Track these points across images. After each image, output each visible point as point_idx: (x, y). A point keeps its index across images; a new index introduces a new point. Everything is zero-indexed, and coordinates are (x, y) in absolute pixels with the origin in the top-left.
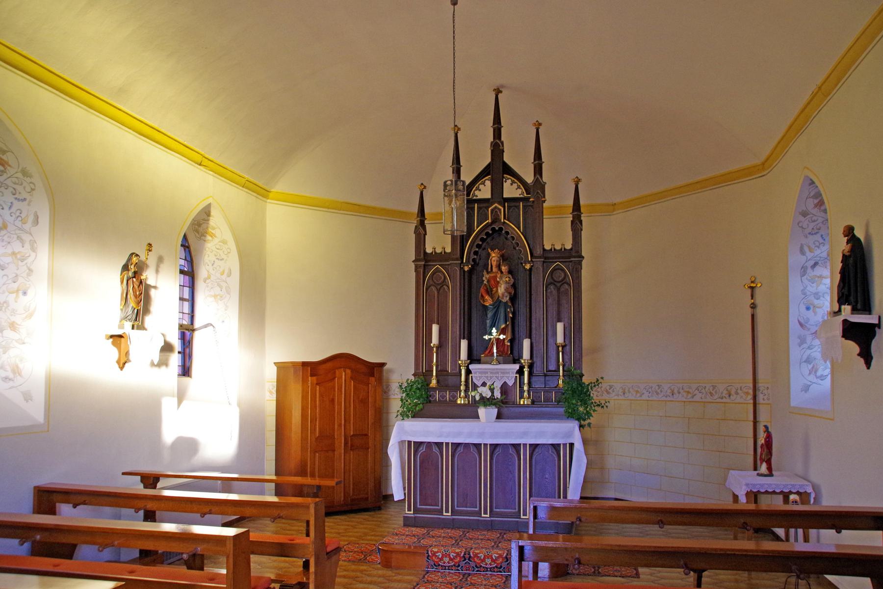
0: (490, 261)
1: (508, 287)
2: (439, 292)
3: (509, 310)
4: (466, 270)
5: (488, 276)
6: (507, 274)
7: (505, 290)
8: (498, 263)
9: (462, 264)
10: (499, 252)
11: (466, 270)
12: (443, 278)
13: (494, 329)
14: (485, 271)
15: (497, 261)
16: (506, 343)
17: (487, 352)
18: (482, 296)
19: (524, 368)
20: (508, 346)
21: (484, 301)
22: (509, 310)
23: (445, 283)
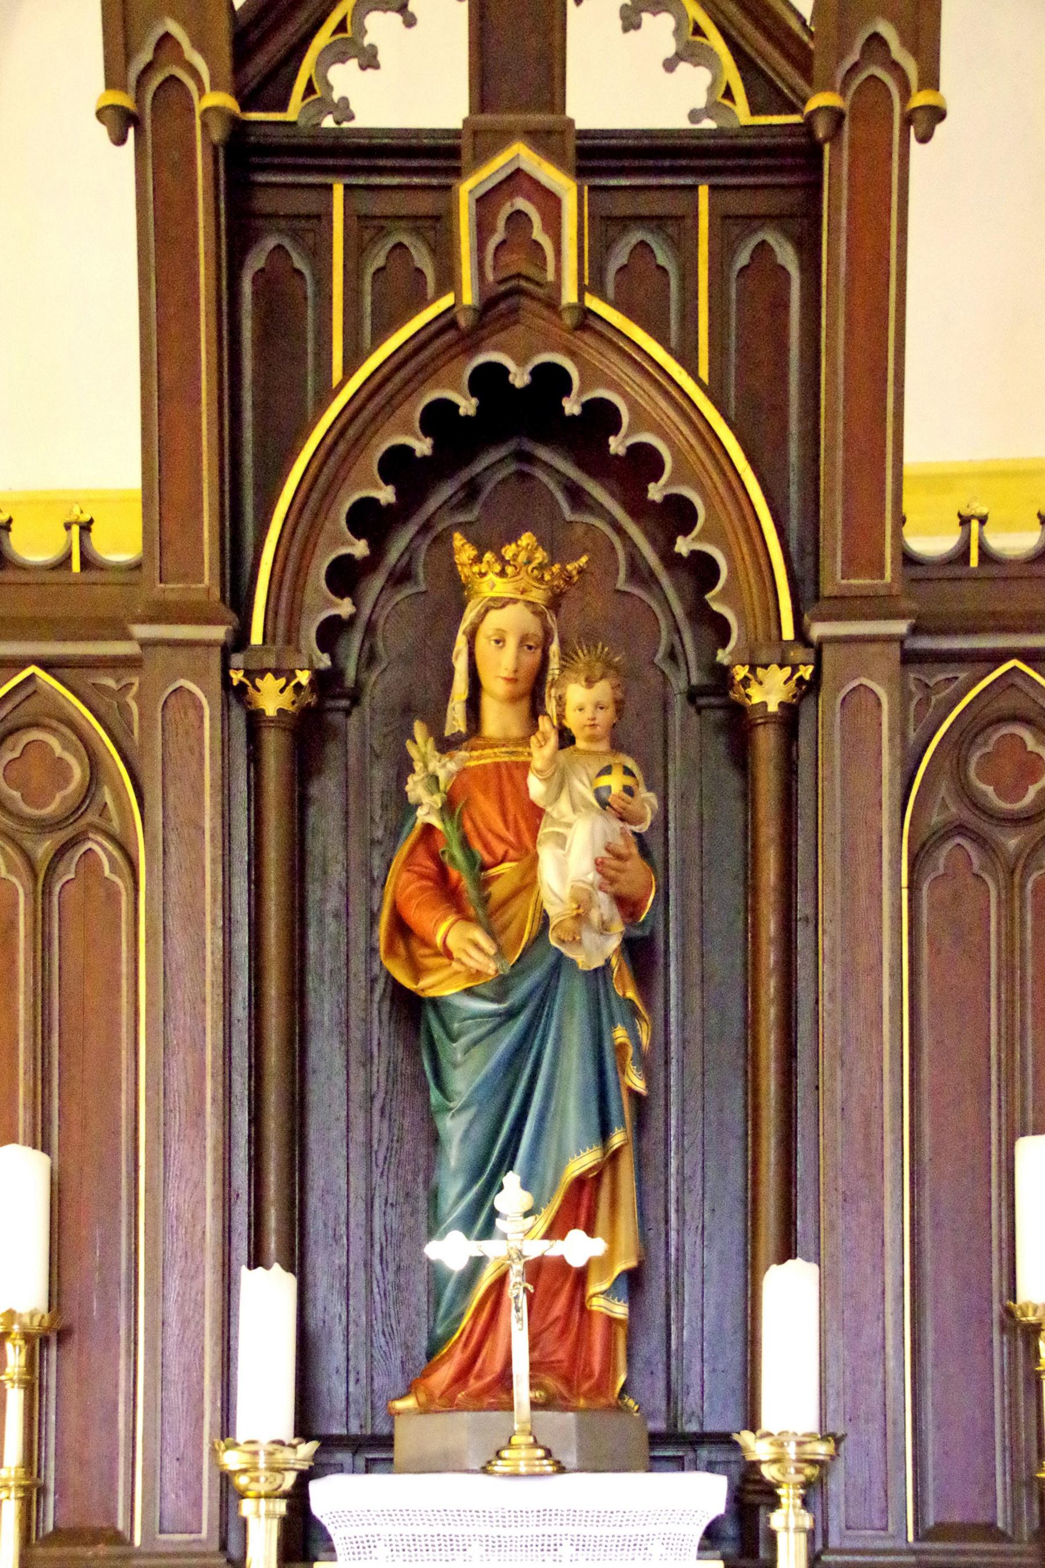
0: (461, 643)
1: (619, 843)
2: (47, 892)
3: (620, 1034)
4: (271, 711)
5: (445, 768)
6: (603, 746)
7: (599, 865)
8: (532, 659)
9: (237, 659)
10: (540, 556)
11: (271, 711)
12: (78, 773)
13: (511, 1180)
14: (419, 729)
15: (523, 641)
16: (597, 1304)
17: (445, 1373)
18: (401, 928)
19: (775, 1503)
20: (611, 1322)
21: (417, 971)
22: (620, 1034)
23: (91, 817)
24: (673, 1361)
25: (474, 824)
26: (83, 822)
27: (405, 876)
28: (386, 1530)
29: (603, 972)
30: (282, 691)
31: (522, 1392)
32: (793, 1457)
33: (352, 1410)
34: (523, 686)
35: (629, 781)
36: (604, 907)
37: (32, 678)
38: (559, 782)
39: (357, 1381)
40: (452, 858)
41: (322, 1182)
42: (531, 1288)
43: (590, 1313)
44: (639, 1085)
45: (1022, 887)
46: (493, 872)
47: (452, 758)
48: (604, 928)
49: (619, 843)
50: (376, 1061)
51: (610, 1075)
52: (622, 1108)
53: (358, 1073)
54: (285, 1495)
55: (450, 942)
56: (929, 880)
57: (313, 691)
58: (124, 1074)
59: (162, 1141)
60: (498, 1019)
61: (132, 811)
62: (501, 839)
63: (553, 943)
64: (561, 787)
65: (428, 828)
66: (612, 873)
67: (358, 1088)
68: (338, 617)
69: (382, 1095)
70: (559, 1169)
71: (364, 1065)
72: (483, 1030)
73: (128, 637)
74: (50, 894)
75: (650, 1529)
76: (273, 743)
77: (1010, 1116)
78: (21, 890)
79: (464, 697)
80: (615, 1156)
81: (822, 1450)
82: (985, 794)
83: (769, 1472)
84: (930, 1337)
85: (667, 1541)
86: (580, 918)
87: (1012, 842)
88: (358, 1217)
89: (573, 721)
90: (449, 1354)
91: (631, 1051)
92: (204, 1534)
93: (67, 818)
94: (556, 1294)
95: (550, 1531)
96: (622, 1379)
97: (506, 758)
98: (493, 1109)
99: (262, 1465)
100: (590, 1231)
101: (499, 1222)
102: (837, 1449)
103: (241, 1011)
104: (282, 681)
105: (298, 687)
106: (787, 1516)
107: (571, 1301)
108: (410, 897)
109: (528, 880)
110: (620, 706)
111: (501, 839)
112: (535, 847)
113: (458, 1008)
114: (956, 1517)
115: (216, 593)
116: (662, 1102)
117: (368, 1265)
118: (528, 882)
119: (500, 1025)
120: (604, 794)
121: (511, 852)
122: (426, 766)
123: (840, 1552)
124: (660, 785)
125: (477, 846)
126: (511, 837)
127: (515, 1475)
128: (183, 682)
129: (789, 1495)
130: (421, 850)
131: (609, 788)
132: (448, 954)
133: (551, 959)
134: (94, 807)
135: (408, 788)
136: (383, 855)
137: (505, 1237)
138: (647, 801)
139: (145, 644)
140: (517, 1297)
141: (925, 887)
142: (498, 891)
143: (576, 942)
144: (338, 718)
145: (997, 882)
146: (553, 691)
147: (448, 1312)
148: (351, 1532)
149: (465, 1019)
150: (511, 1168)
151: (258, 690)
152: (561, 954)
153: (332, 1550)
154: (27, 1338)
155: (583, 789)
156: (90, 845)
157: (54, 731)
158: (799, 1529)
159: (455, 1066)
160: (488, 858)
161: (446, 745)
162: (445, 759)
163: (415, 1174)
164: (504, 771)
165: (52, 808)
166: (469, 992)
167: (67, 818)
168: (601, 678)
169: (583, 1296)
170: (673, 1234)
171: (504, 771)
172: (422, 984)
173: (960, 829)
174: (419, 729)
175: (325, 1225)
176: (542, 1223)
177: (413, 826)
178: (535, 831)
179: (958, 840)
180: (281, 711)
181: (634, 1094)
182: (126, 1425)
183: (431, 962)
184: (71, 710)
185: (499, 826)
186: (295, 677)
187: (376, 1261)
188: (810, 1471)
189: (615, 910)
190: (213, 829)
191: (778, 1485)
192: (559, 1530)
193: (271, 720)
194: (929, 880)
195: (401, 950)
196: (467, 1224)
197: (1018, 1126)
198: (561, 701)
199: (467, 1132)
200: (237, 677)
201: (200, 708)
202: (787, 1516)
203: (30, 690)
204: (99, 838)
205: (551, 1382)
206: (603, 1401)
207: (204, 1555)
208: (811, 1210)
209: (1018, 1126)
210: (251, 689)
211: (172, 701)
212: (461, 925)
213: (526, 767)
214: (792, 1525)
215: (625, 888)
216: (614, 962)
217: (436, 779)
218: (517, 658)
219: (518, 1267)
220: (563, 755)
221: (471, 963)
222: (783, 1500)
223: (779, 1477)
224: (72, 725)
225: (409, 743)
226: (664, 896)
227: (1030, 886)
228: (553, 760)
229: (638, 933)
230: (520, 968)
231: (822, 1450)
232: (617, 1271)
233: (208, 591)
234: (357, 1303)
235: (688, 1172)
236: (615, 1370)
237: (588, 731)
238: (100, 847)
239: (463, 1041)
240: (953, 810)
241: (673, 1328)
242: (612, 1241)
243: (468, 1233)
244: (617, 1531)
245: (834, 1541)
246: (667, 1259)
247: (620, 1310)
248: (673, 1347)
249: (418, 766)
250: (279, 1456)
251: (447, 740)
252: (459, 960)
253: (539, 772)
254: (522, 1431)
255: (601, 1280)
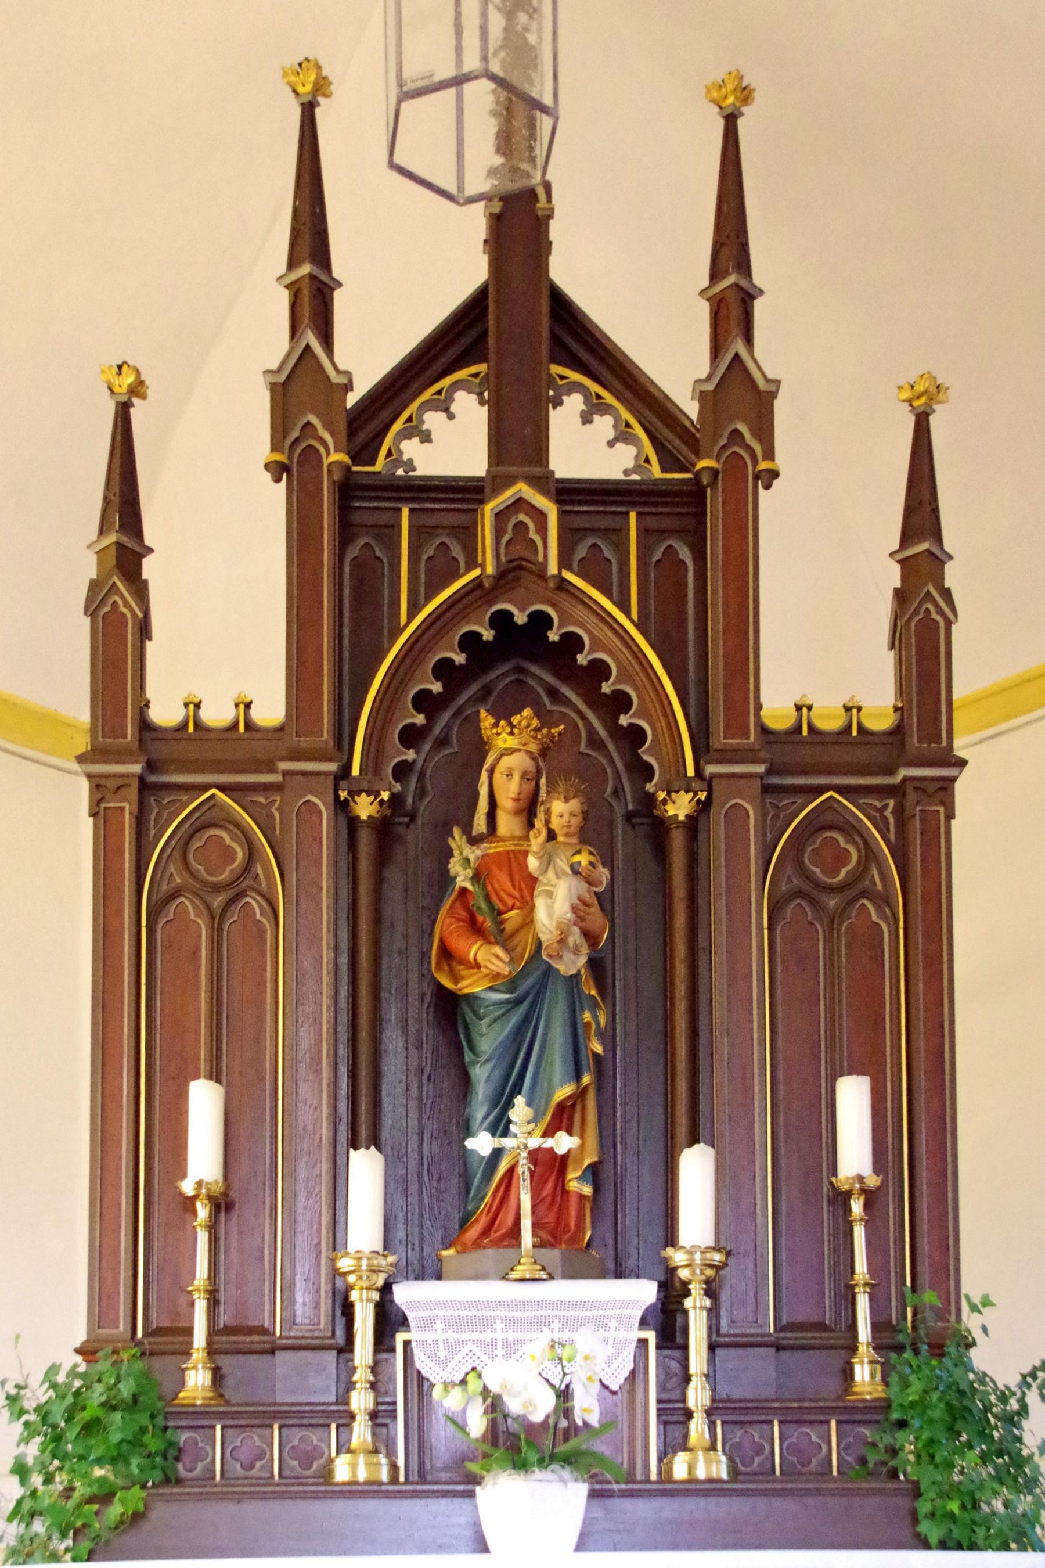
0: (484, 776)
1: (587, 897)
2: (220, 930)
3: (587, 1016)
4: (364, 817)
5: (473, 854)
6: (574, 840)
7: (574, 909)
8: (530, 786)
9: (343, 784)
10: (535, 723)
11: (364, 817)
12: (240, 855)
13: (520, 1101)
14: (457, 832)
15: (524, 775)
16: (573, 1186)
17: (473, 1232)
18: (446, 954)
19: (687, 1293)
20: (582, 1197)
21: (456, 979)
22: (587, 1016)
23: (248, 882)
24: (619, 1238)
25: (493, 887)
26: (244, 885)
27: (448, 921)
28: (441, 1313)
29: (575, 978)
30: (371, 804)
31: (527, 1238)
32: (698, 1262)
33: (410, 1269)
34: (523, 804)
35: (592, 858)
36: (575, 937)
37: (213, 796)
38: (548, 860)
39: (413, 1249)
40: (479, 908)
41: (390, 1122)
42: (532, 1167)
43: (568, 1192)
44: (598, 1048)
45: (839, 930)
46: (505, 916)
47: (478, 848)
48: (576, 951)
49: (587, 897)
50: (425, 1046)
51: (581, 1039)
52: (586, 1061)
53: (413, 1052)
54: (377, 1289)
55: (479, 958)
56: (782, 924)
57: (389, 807)
58: (268, 1043)
59: (293, 1081)
60: (509, 1006)
61: (274, 877)
62: (510, 895)
63: (545, 958)
64: (549, 863)
65: (464, 891)
66: (582, 914)
67: (414, 1063)
68: (405, 761)
69: (428, 1068)
70: (549, 1096)
71: (417, 1048)
72: (499, 1012)
73: (272, 770)
74: (222, 930)
75: (609, 1312)
76: (365, 840)
77: (833, 1062)
78: (203, 927)
79: (486, 810)
80: (585, 1089)
81: (718, 1257)
82: (814, 873)
83: (684, 1274)
84: (783, 1206)
85: (620, 1319)
86: (562, 941)
87: (832, 902)
88: (413, 1144)
89: (555, 823)
90: (477, 1220)
91: (594, 1026)
92: (322, 1326)
93: (233, 883)
94: (546, 1182)
95: (547, 1313)
96: (588, 1234)
97: (513, 848)
98: (504, 1064)
99: (364, 1268)
100: (570, 1133)
101: (512, 1127)
102: (727, 1259)
103: (343, 1004)
104: (372, 798)
105: (382, 801)
106: (695, 1300)
107: (555, 1189)
108: (451, 933)
109: (528, 920)
110: (585, 815)
111: (510, 895)
112: (532, 898)
113: (484, 999)
114: (800, 1318)
115: (331, 742)
116: (611, 1073)
117: (420, 1176)
118: (529, 920)
119: (508, 1011)
120: (576, 867)
121: (517, 904)
122: (461, 853)
123: (728, 1335)
124: (609, 862)
125: (495, 899)
126: (516, 894)
127: (523, 1280)
128: (310, 797)
129: (696, 1289)
130: (458, 905)
131: (579, 863)
132: (478, 966)
133: (543, 967)
134: (250, 876)
135: (450, 866)
136: (429, 916)
137: (515, 1136)
138: (603, 874)
139: (286, 774)
140: (523, 1173)
141: (779, 928)
142: (509, 927)
143: (560, 957)
144: (401, 830)
145: (822, 924)
146: (542, 808)
147: (476, 1195)
148: (420, 1314)
149: (488, 1006)
150: (519, 1093)
151: (356, 803)
152: (550, 965)
153: (408, 1326)
154: (210, 1198)
155: (563, 864)
156: (248, 899)
157: (226, 829)
158: (702, 1308)
159: (482, 1035)
160: (502, 907)
161: (474, 841)
162: (474, 848)
163: (450, 1118)
164: (512, 856)
165: (224, 876)
166: (491, 989)
167: (233, 883)
168: (574, 797)
169: (563, 1182)
170: (619, 1157)
171: (512, 856)
172: (460, 985)
173: (800, 894)
174: (457, 832)
175: (392, 1149)
176: (539, 1131)
177: (453, 890)
178: (532, 891)
179: (798, 901)
180: (370, 817)
181: (596, 1055)
182: (270, 1262)
183: (464, 973)
184: (239, 817)
185: (508, 885)
186: (380, 795)
187: (425, 1173)
188: (710, 1272)
189: (583, 938)
190: (328, 887)
191: (689, 1282)
192: (551, 1313)
193: (364, 822)
194: (782, 924)
195: (446, 968)
196: (493, 1131)
197: (838, 1068)
198: (548, 812)
199: (489, 1077)
200: (343, 795)
201: (320, 812)
202: (695, 1300)
203: (212, 803)
204: (254, 895)
205: (544, 1235)
206: (576, 1246)
207: (323, 1338)
208: (708, 1125)
209: (838, 1068)
210: (352, 804)
211: (303, 808)
212: (485, 947)
213: (526, 853)
214: (698, 1305)
215: (588, 925)
216: (583, 972)
217: (467, 860)
218: (521, 785)
219: (524, 1154)
220: (549, 845)
221: (493, 968)
222: (693, 1291)
223: (690, 1277)
224: (238, 825)
225: (450, 840)
226: (612, 937)
227: (843, 928)
228: (543, 847)
229: (596, 955)
230: (524, 973)
231: (718, 1257)
232: (586, 1163)
233: (326, 741)
234: (413, 1199)
235: (628, 1117)
236: (584, 1228)
237: (565, 830)
238: (254, 902)
239: (487, 1020)
240: (795, 882)
241: (619, 1216)
242: (582, 1137)
243: (494, 1135)
244: (588, 1313)
245: (724, 1329)
246: (616, 1174)
247: (587, 1190)
248: (619, 1229)
249: (456, 853)
250: (375, 1262)
251: (475, 837)
252: (486, 967)
253: (536, 853)
254: (527, 1256)
255: (575, 1170)
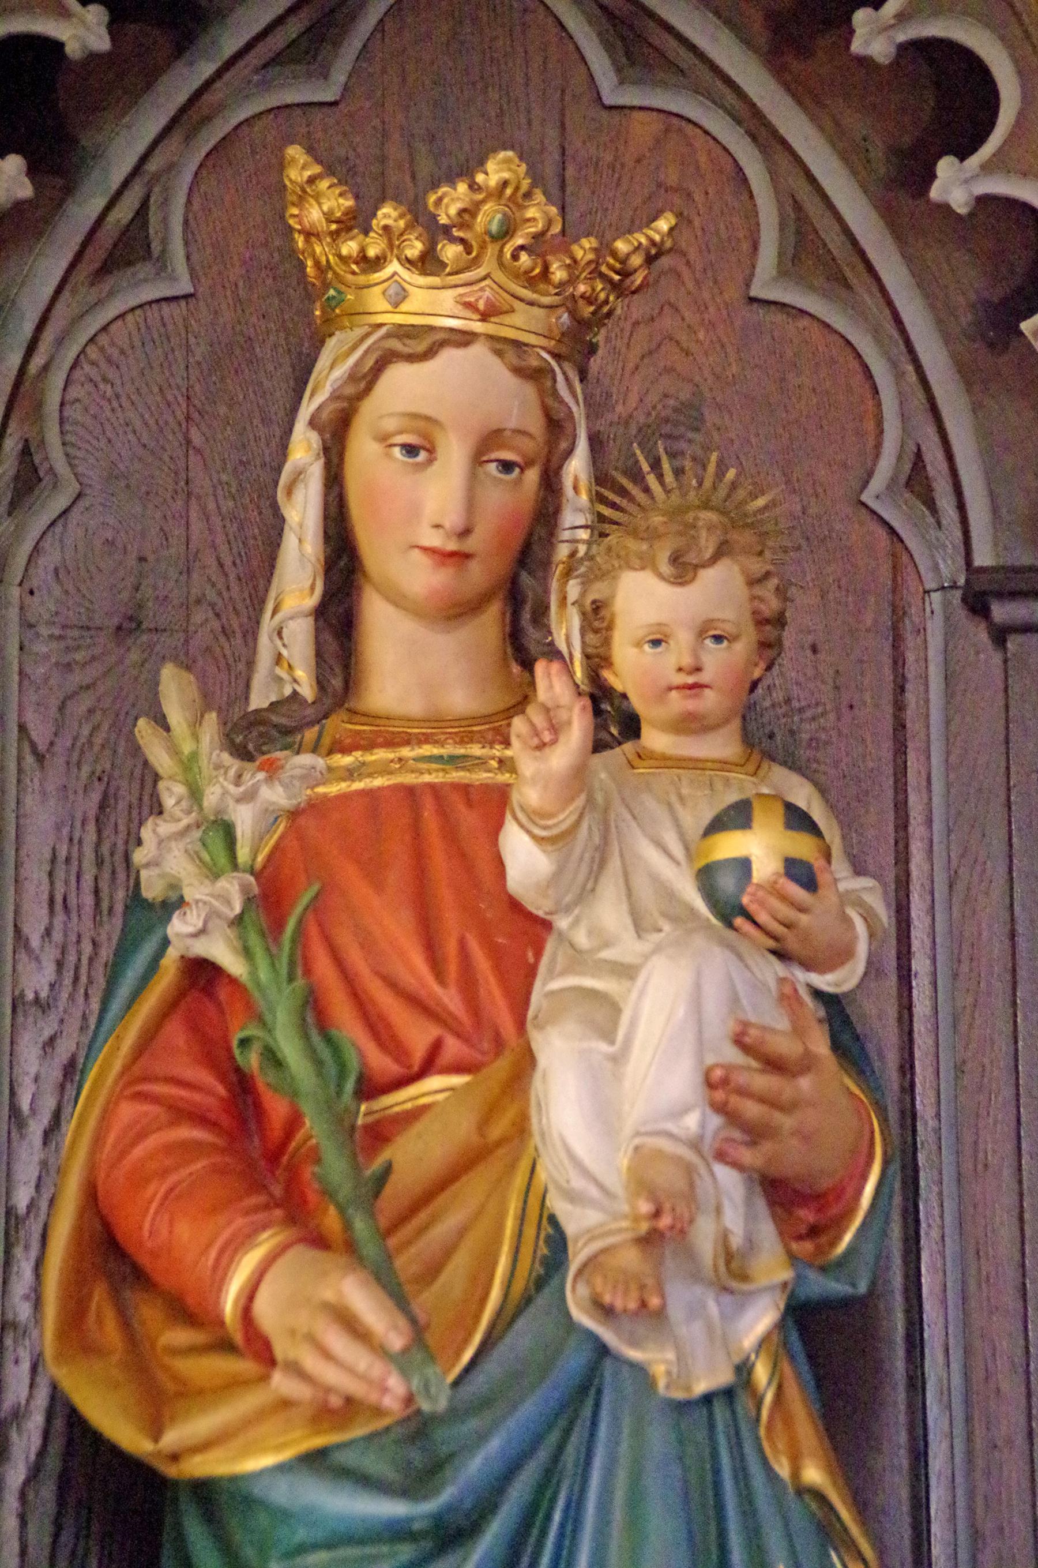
35: (802, 846)
40: (273, 1058)
47: (272, 770)
66: (752, 1110)
120: (727, 883)
121: (453, 1047)
122: (195, 794)
126: (450, 999)
130: (176, 1033)
131: (744, 865)
146: (573, 590)
160: (382, 1063)
177: (154, 966)
249: (172, 793)
251: (257, 720)
